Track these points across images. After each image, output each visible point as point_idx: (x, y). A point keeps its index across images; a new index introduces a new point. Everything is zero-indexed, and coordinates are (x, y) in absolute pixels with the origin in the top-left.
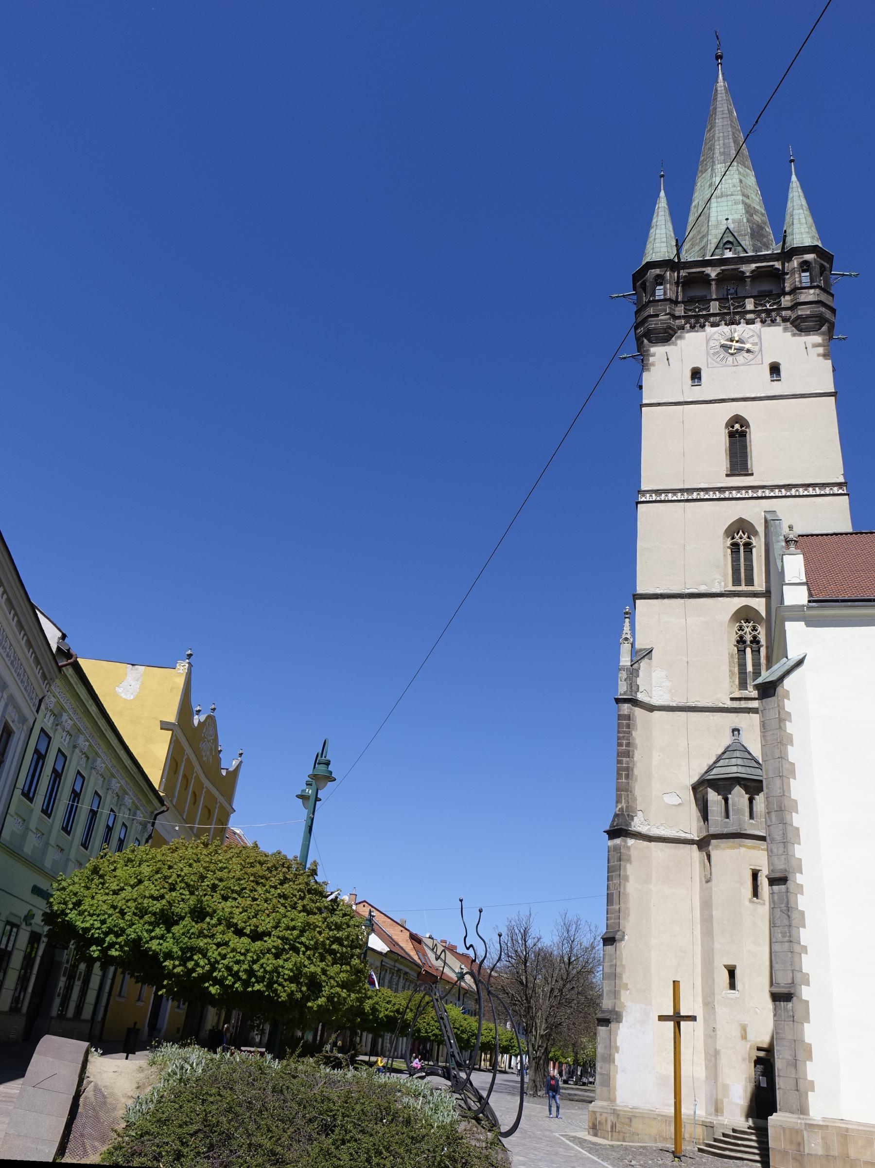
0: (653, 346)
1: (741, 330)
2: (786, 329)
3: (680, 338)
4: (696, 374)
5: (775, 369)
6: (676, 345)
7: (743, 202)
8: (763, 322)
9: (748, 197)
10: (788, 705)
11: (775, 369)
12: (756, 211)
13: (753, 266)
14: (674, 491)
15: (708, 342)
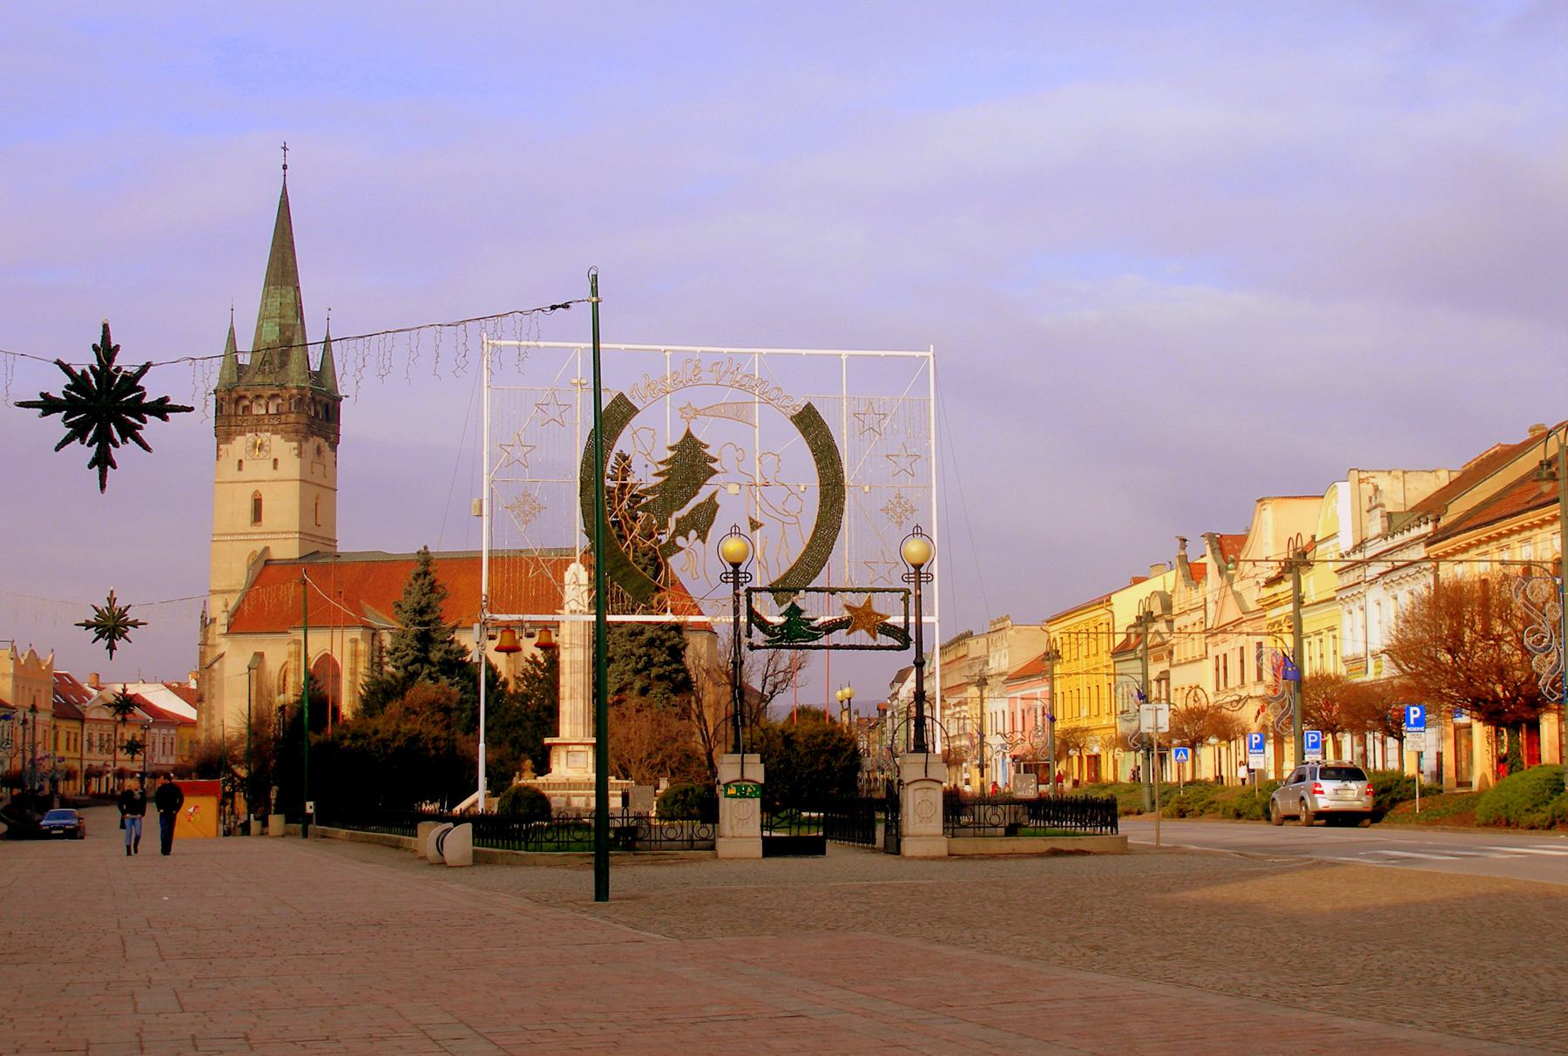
0: (221, 444)
1: (261, 435)
2: (282, 437)
3: (234, 439)
4: (240, 461)
5: (276, 460)
6: (231, 443)
7: (280, 325)
8: (272, 430)
9: (284, 317)
10: (213, 674)
11: (276, 460)
12: (289, 325)
13: (270, 392)
14: (227, 535)
15: (247, 442)
